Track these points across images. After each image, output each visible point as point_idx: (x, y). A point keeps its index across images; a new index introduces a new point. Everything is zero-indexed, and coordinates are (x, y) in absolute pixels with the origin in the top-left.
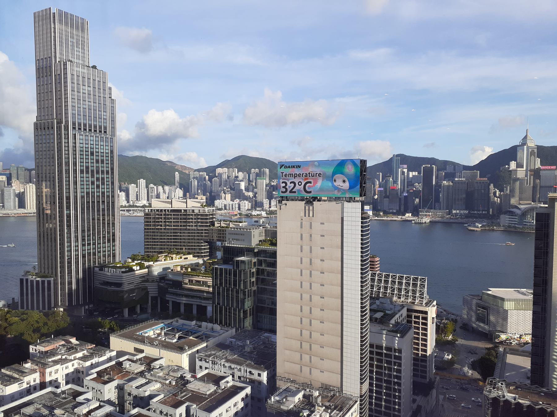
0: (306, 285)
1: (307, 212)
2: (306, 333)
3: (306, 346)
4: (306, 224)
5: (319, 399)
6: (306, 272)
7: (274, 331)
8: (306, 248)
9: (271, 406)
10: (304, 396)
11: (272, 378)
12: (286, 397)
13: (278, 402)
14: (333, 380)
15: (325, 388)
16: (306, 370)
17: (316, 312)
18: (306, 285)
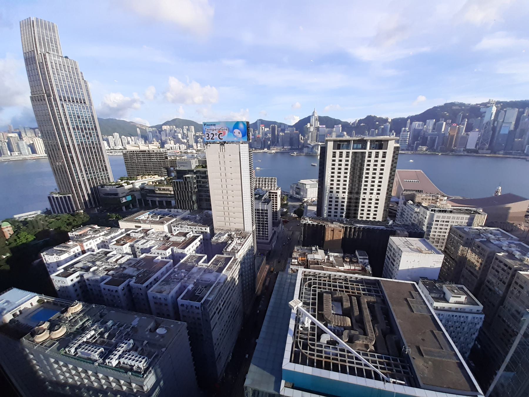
0: (224, 186)
1: (221, 149)
2: (226, 208)
3: (226, 214)
4: (222, 156)
5: (235, 235)
6: (224, 180)
7: (211, 209)
8: (223, 168)
9: (214, 242)
10: (228, 235)
11: (212, 230)
12: (220, 237)
13: (216, 239)
14: (240, 227)
15: (237, 230)
16: (228, 224)
17: (230, 198)
18: (224, 186)
